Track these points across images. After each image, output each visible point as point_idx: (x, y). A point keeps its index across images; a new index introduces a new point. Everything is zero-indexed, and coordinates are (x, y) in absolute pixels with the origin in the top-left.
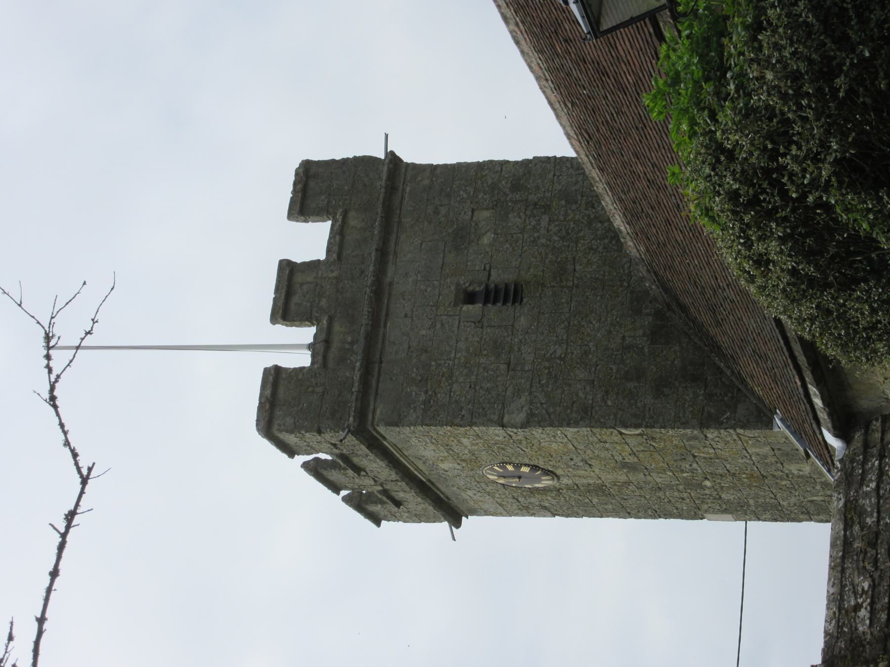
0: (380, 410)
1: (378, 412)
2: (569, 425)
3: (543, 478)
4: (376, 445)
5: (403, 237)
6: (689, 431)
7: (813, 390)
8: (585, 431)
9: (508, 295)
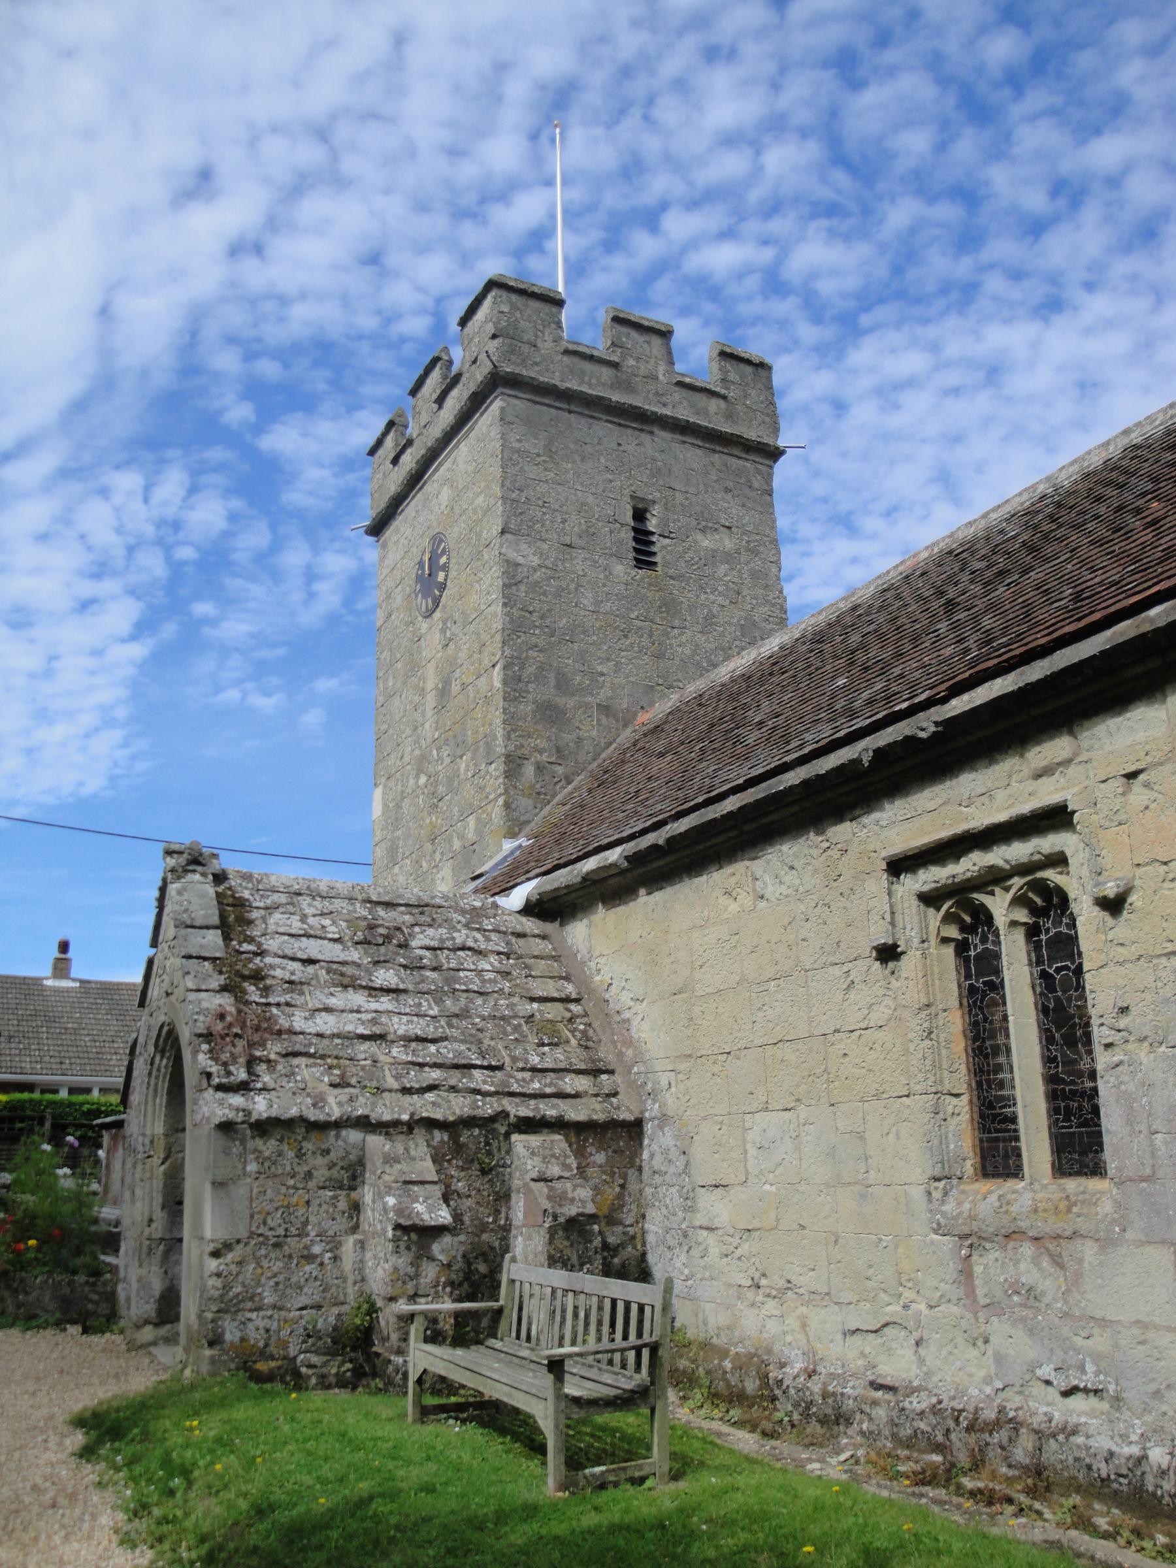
0: (519, 404)
1: (516, 402)
2: (505, 605)
3: (430, 600)
4: (477, 402)
5: (699, 452)
6: (500, 741)
7: (614, 855)
8: (498, 625)
9: (643, 556)
